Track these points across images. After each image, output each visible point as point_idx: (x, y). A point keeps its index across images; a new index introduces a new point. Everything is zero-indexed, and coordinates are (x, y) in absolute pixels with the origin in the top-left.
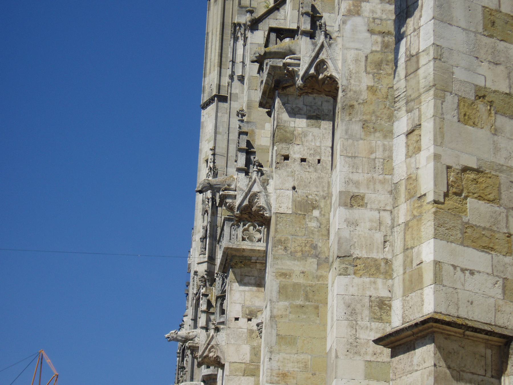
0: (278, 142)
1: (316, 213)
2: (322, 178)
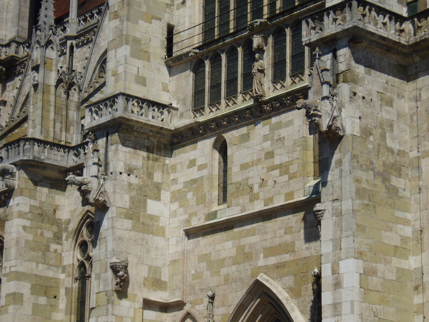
0: (351, 82)
1: (371, 138)
2: (374, 113)
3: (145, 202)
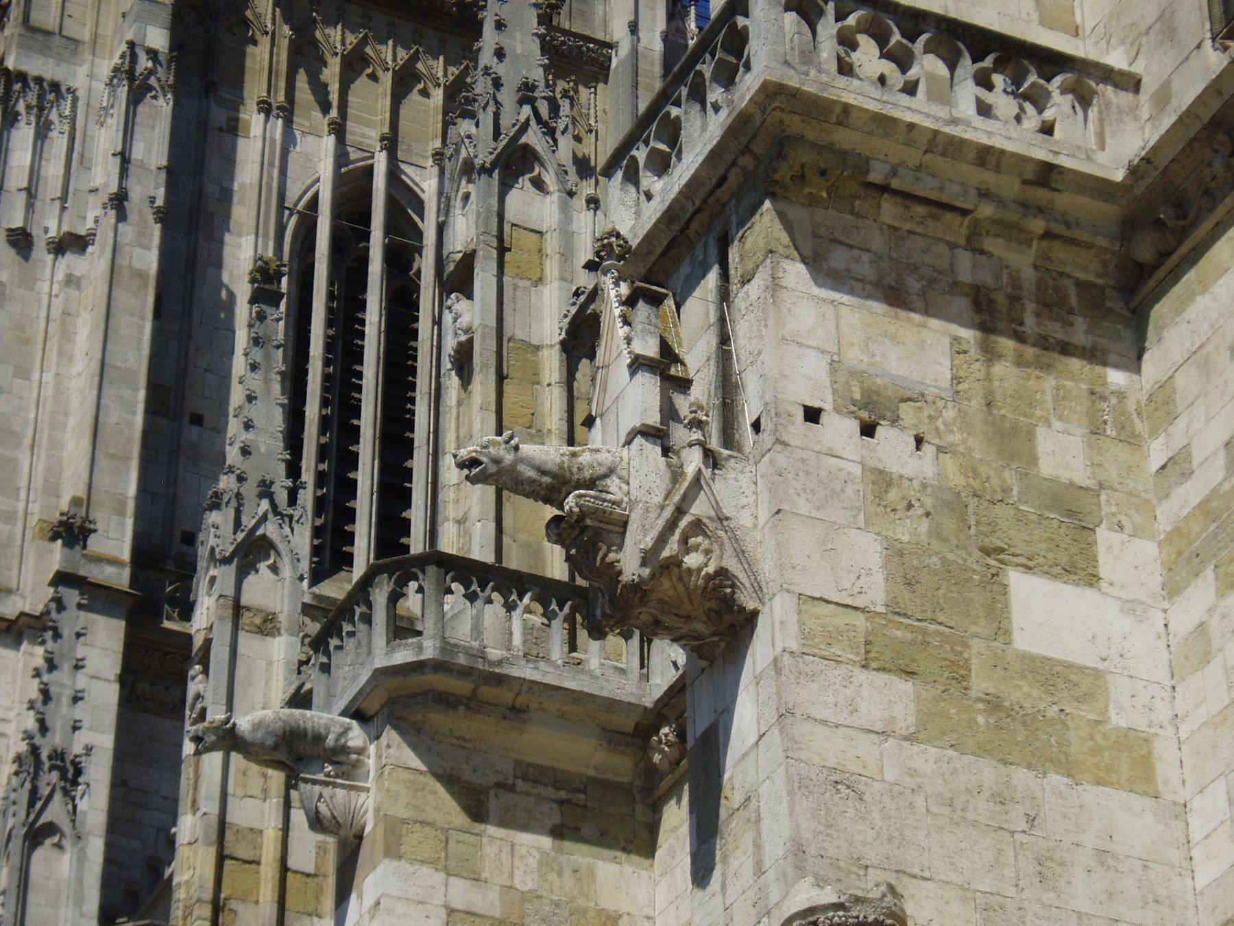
3: (995, 585)
